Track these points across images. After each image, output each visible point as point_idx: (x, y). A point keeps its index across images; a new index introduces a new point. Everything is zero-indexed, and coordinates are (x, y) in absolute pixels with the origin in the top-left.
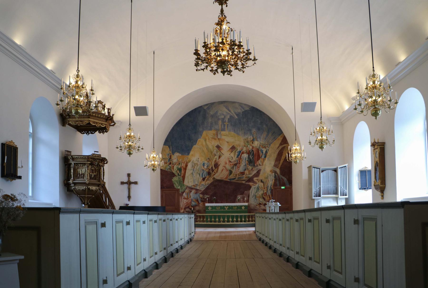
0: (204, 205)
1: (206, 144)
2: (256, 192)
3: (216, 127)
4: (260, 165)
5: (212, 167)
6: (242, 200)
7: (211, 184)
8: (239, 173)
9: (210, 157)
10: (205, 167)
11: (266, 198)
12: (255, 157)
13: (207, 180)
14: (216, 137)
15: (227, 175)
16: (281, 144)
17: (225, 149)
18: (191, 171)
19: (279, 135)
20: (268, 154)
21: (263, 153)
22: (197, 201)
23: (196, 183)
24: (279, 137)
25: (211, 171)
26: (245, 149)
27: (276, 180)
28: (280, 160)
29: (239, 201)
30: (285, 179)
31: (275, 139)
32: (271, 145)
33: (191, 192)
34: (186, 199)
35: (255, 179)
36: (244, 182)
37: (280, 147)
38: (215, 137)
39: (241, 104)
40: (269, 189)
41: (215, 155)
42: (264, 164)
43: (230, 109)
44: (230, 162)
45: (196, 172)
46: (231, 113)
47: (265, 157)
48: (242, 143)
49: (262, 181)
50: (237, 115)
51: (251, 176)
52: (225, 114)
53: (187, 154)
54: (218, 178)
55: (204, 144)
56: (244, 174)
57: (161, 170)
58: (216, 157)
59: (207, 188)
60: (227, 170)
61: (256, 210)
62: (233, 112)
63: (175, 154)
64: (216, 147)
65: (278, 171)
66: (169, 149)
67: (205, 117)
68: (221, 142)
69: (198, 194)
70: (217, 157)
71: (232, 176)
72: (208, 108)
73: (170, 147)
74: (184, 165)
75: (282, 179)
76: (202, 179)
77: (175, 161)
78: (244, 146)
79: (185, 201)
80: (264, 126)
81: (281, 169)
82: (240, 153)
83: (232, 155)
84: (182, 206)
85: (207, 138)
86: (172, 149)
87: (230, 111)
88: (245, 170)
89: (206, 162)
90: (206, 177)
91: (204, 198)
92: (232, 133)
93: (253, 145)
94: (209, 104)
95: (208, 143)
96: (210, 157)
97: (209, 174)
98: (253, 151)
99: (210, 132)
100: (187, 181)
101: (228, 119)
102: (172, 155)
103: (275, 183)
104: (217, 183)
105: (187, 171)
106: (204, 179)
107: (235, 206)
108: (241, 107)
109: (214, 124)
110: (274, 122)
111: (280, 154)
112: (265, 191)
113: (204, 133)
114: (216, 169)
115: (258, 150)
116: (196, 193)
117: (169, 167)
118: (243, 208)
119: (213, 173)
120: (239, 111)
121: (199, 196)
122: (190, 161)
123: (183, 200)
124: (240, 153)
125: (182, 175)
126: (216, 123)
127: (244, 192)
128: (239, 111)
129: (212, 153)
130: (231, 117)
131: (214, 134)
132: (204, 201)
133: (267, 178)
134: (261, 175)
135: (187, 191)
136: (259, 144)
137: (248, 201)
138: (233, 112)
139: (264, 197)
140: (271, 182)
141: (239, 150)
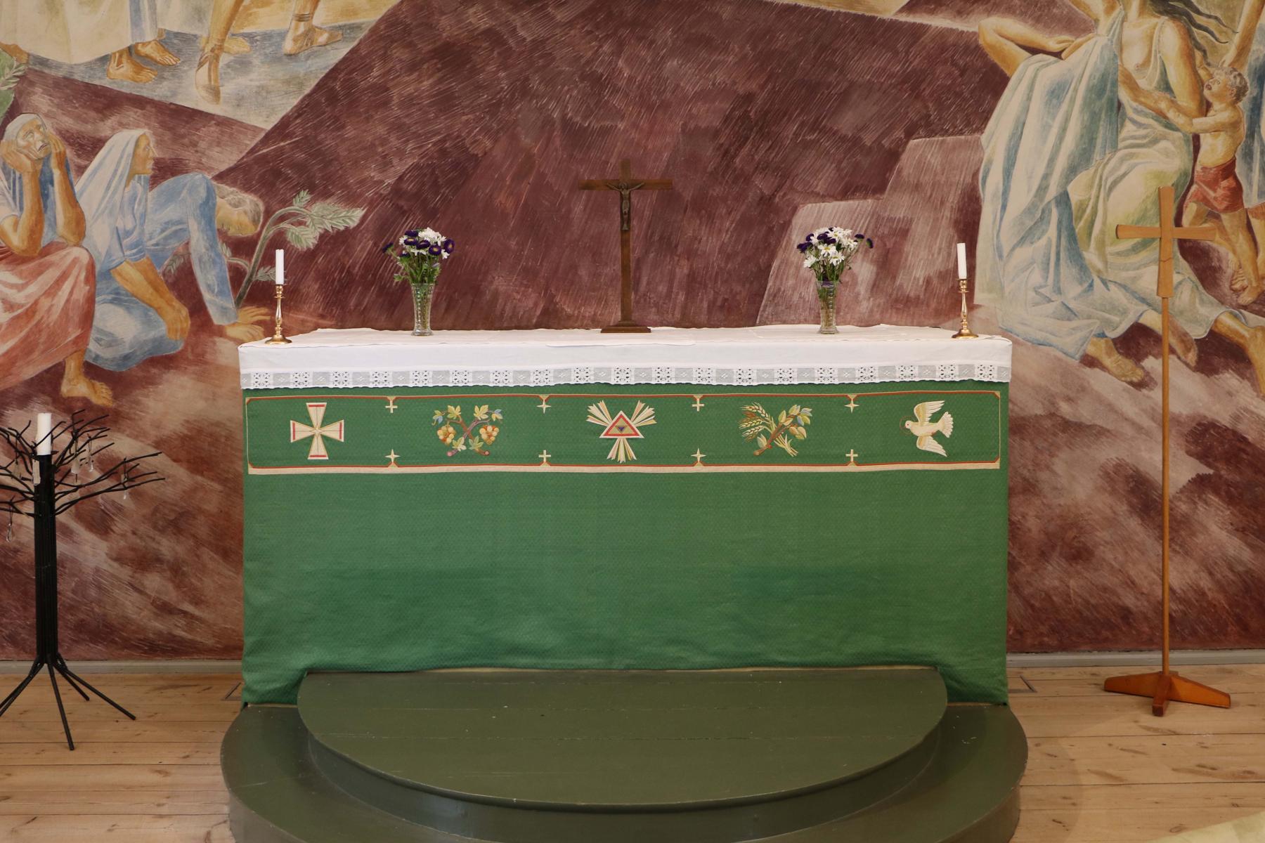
6: (864, 271)
22: (183, 284)
23: (174, 21)
29: (829, 300)
33: (89, 147)
59: (335, 97)
61: (1074, 429)
69: (195, 182)
107: (775, 396)
112: (1214, 151)
116: (165, 170)
118: (928, 427)
121: (207, 208)
127: (894, 155)
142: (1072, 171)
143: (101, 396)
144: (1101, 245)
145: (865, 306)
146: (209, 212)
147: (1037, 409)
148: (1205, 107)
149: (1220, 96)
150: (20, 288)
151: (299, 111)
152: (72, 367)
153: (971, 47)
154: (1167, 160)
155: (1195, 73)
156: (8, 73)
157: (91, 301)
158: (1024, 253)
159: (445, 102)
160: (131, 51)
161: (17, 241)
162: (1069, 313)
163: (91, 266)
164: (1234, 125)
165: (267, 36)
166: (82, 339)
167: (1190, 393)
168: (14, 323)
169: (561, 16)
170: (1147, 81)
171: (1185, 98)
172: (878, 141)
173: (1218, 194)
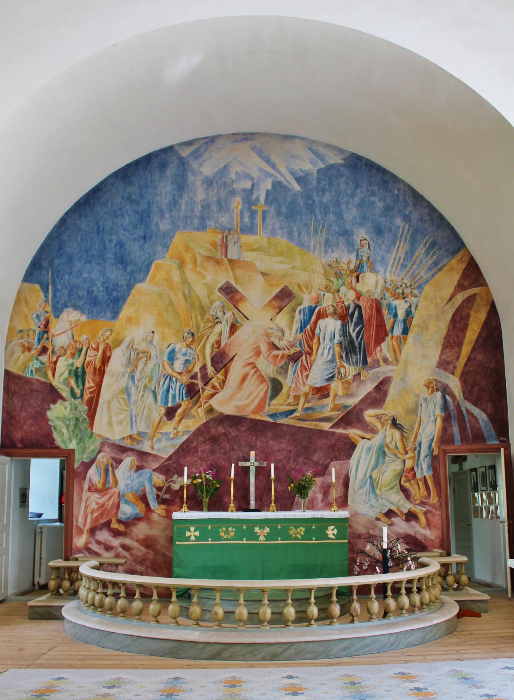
0: (168, 515)
1: (185, 281)
2: (376, 466)
3: (224, 219)
4: (386, 360)
5: (204, 368)
7: (199, 432)
8: (306, 389)
10: (178, 365)
11: (414, 490)
12: (366, 331)
13: (183, 416)
14: (220, 255)
15: (263, 400)
16: (460, 287)
17: (256, 295)
18: (124, 382)
19: (454, 253)
20: (415, 322)
21: (395, 316)
22: (144, 499)
23: (142, 429)
24: (454, 261)
25: (200, 383)
26: (328, 302)
27: (447, 419)
28: (460, 345)
30: (482, 417)
31: (437, 266)
32: (427, 288)
33: (119, 462)
34: (97, 490)
35: (369, 414)
36: (326, 426)
37: (460, 298)
38: (219, 255)
39: (311, 145)
40: (423, 454)
41: (216, 321)
42: (403, 356)
43: (273, 159)
45: (141, 385)
46: (278, 172)
47: (405, 331)
48: (319, 281)
49: (394, 423)
50: (298, 180)
51: (352, 402)
52: (255, 174)
53: (108, 314)
54: (228, 410)
55: (176, 277)
56: (328, 396)
57: (7, 373)
58: (218, 328)
59: (185, 449)
60: (262, 379)
62: (284, 171)
63: (64, 315)
64: (221, 289)
65: (454, 383)
66: (42, 295)
67: (181, 185)
68: (239, 272)
69: (147, 472)
70: (224, 328)
71: (279, 404)
72: (196, 155)
73: (45, 289)
74: (94, 357)
75: (472, 415)
76: (163, 411)
78: (327, 289)
79: (95, 500)
80: (399, 222)
81: (464, 378)
82: (314, 315)
84: (81, 520)
85: (188, 258)
86: (55, 296)
88: (331, 379)
89: (180, 347)
90: (179, 406)
91: (169, 490)
92: (283, 241)
93: (359, 287)
94: (197, 140)
95: (190, 275)
96: (198, 327)
97: (192, 391)
98: (358, 307)
99: (200, 234)
101: (268, 193)
102: (52, 318)
103: (444, 430)
104: (225, 431)
105: (106, 379)
106: (170, 413)
108: (316, 153)
109: (214, 208)
110: (432, 209)
111: (459, 322)
112: (409, 464)
113: (179, 239)
114: (220, 376)
116: (139, 468)
117: (37, 365)
119: (209, 390)
121: (150, 479)
122: (118, 343)
123: (86, 494)
124: (314, 315)
125: (86, 397)
126: (223, 206)
128: (307, 165)
129: (203, 311)
130: (277, 185)
131: (214, 245)
132: (171, 499)
133: (414, 411)
134: (389, 399)
135: (103, 458)
136: (381, 282)
137: (343, 503)
138: (284, 171)
139: (407, 485)
140: (429, 429)
141: (306, 304)
142: (373, 470)
143: (122, 528)
144: (380, 489)
146: (151, 480)
147: (364, 531)
148: (406, 453)
149: (410, 450)
150: (100, 499)
151: (174, 453)
152: (114, 520)
154: (397, 466)
155: (404, 444)
156: (98, 442)
157: (119, 503)
158: (361, 491)
159: (213, 452)
160: (130, 436)
161: (100, 486)
162: (373, 507)
163: (119, 494)
164: (414, 457)
165: (166, 433)
166: (116, 513)
167: (402, 526)
168: (99, 508)
169: (242, 429)
170: (392, 446)
171: (402, 451)
172: (323, 463)
173: (410, 475)
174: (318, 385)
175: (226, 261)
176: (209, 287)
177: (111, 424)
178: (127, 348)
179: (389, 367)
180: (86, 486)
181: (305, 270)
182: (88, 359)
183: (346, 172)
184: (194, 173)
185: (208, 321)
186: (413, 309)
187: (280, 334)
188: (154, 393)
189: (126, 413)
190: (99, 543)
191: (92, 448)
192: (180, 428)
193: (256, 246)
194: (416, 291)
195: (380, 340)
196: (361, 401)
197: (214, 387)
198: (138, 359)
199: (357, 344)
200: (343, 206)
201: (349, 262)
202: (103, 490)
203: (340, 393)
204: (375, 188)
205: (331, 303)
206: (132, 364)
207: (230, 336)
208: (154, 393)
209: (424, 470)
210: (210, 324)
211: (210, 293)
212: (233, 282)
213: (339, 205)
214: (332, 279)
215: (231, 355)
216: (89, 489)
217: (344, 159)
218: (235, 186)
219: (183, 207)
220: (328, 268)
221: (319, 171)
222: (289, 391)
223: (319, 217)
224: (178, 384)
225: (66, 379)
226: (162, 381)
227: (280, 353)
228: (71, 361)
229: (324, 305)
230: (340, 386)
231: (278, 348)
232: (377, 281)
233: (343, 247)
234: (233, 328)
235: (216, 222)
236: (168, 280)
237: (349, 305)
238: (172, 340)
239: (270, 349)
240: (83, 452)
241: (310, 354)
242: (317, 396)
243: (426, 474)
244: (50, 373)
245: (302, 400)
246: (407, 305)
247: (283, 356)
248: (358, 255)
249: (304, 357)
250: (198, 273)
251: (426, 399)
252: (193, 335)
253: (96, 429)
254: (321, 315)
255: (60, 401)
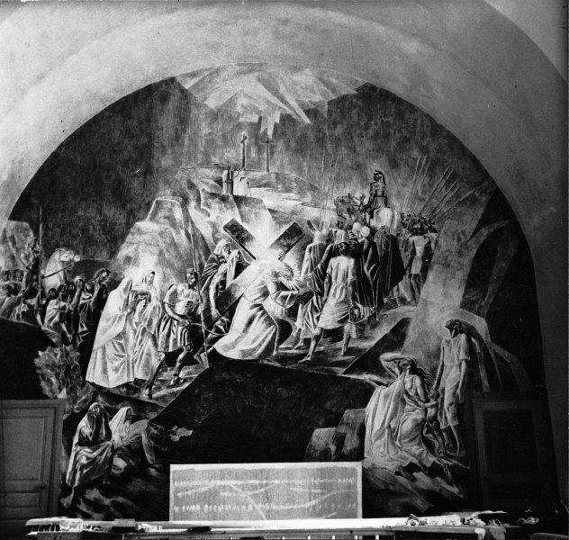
1: (187, 218)
4: (403, 301)
5: (207, 310)
8: (317, 332)
9: (201, 266)
12: (381, 271)
16: (484, 222)
17: (264, 233)
21: (414, 252)
23: (140, 375)
35: (386, 357)
36: (340, 372)
37: (485, 232)
44: (281, 287)
45: (140, 329)
46: (286, 103)
47: (425, 269)
48: (329, 217)
49: (415, 369)
50: (308, 112)
51: (367, 345)
52: (262, 107)
54: (234, 354)
55: (178, 214)
58: (222, 268)
60: (269, 321)
63: (56, 256)
64: (226, 227)
65: (480, 325)
67: (183, 121)
68: (245, 209)
69: (144, 423)
70: (229, 267)
71: (288, 348)
77: (53, 281)
79: (85, 454)
80: (415, 153)
83: (291, 259)
86: (45, 235)
87: (282, 99)
90: (180, 350)
93: (373, 223)
96: (201, 266)
98: (372, 244)
100: (99, 367)
101: (276, 126)
105: (102, 324)
112: (431, 412)
115: (393, 241)
117: (23, 308)
120: (317, 98)
121: (148, 431)
122: (114, 284)
133: (437, 354)
136: (397, 217)
140: (452, 377)
141: (316, 242)
142: (391, 419)
144: (400, 441)
145: (333, 458)
149: (432, 397)
150: (91, 453)
153: (362, 383)
154: (418, 415)
155: (425, 391)
156: (91, 390)
158: (378, 442)
160: (127, 385)
163: (113, 446)
166: (109, 469)
168: (89, 464)
172: (336, 411)
174: (330, 327)
175: (231, 198)
176: (214, 225)
177: (106, 371)
178: (125, 290)
179: (406, 308)
180: (76, 440)
181: (315, 206)
182: (81, 302)
183: (359, 103)
184: (198, 106)
185: (213, 260)
186: (433, 245)
187: (289, 274)
188: (154, 338)
189: (122, 359)
190: (88, 502)
191: (84, 397)
192: (182, 375)
193: (264, 182)
194: (435, 226)
195: (396, 279)
196: (376, 344)
197: (218, 330)
198: (137, 302)
199: (371, 283)
200: (356, 140)
201: (363, 197)
202: (92, 442)
203: (354, 335)
204: (390, 119)
205: (343, 241)
206: (130, 307)
207: (235, 277)
208: (154, 338)
209: (449, 419)
210: (215, 264)
211: (215, 232)
212: (239, 220)
213: (352, 138)
214: (344, 215)
215: (237, 296)
216: (80, 443)
217: (357, 90)
218: (241, 119)
219: (186, 142)
220: (339, 203)
221: (329, 103)
222: (299, 334)
223: (330, 151)
224: (180, 328)
225: (55, 324)
226: (163, 324)
227: (289, 293)
228: (62, 304)
229: (336, 242)
230: (354, 329)
231: (286, 289)
232: (393, 217)
233: (355, 180)
234: (240, 268)
235: (221, 158)
236: (171, 219)
237: (363, 242)
238: (174, 280)
239: (278, 289)
240: (75, 402)
241: (322, 295)
242: (329, 339)
243: (450, 424)
244: (38, 317)
245: (313, 344)
246: (426, 241)
247: (292, 296)
248: (371, 189)
249: (314, 298)
250: (203, 211)
251: (448, 342)
252: (196, 275)
253: (90, 378)
254: (334, 253)
255: (49, 348)
